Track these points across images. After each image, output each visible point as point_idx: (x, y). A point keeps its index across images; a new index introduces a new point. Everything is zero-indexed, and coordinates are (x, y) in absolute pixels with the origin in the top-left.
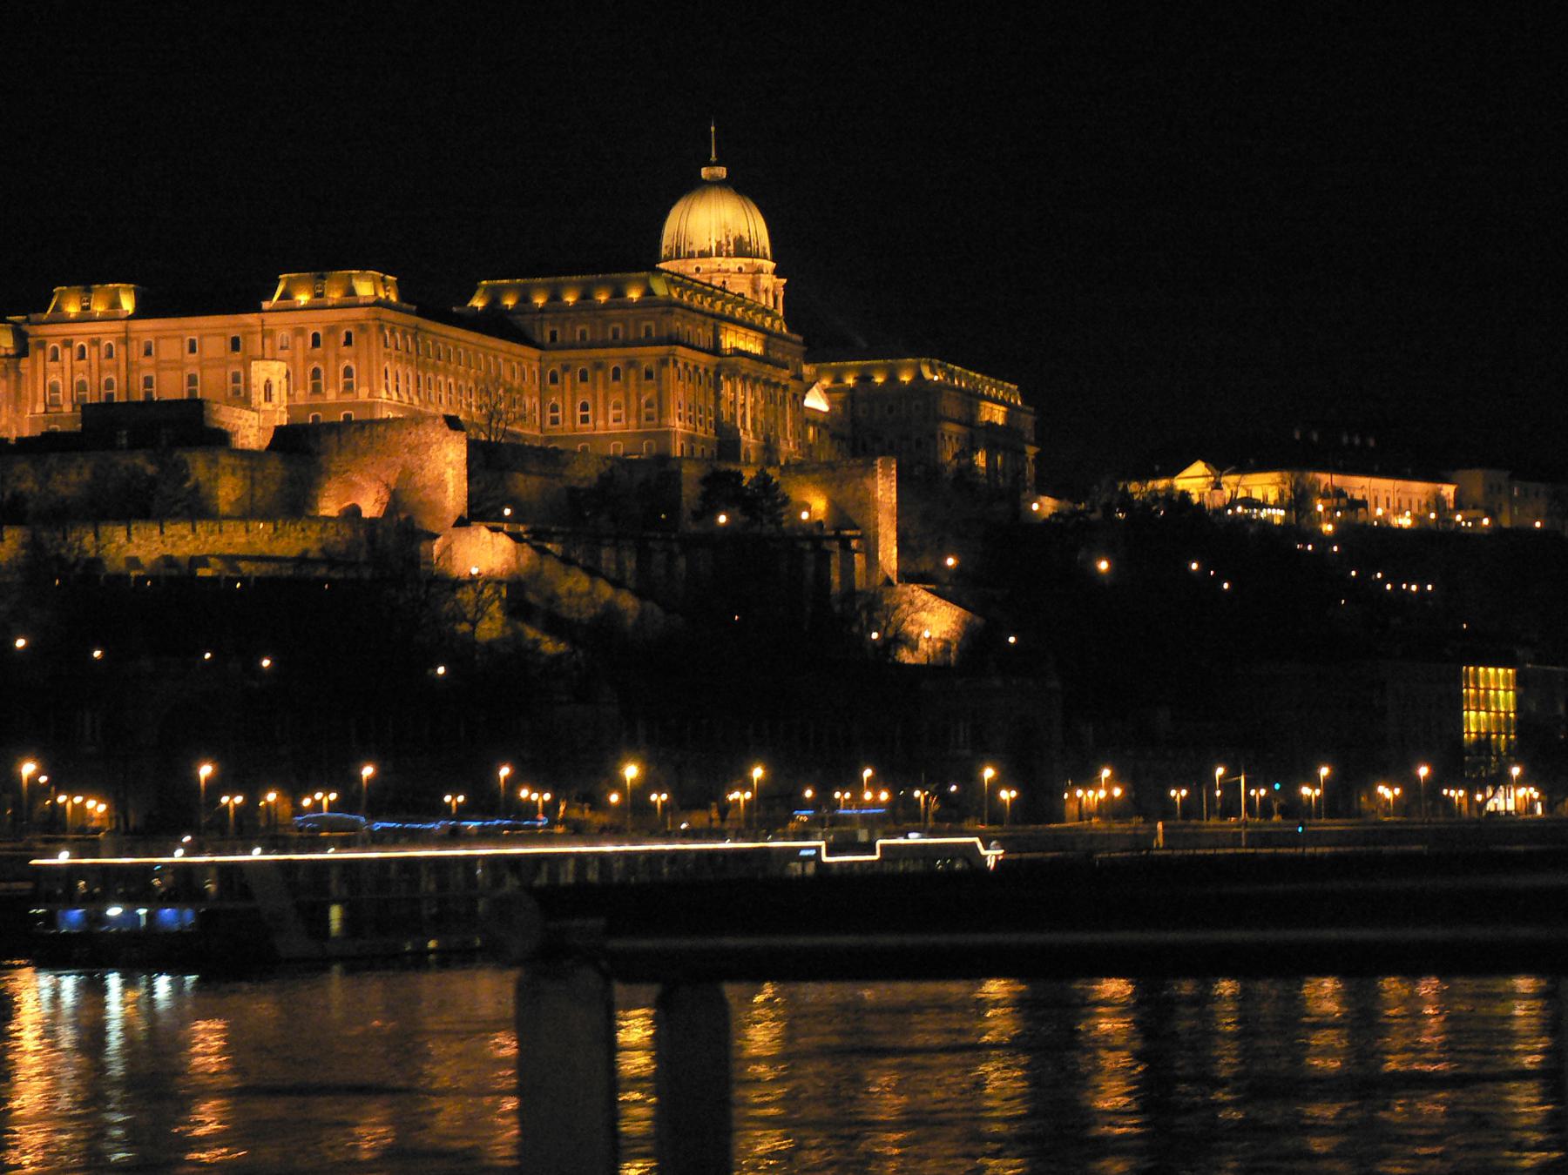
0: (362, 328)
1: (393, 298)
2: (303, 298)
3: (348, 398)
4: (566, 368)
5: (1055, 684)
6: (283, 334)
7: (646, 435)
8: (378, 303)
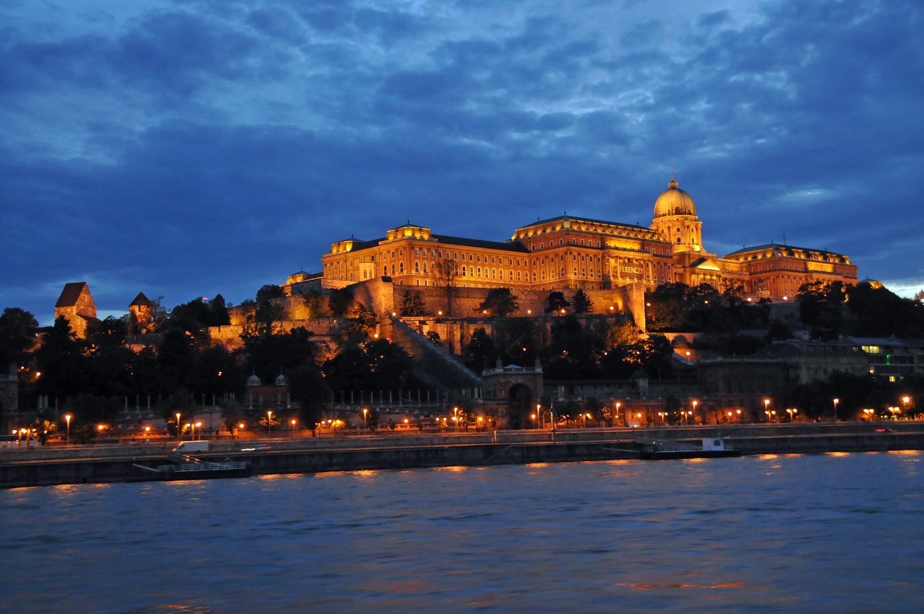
0: (405, 248)
1: (426, 237)
2: (391, 238)
3: (401, 275)
4: (537, 259)
5: (539, 370)
6: (384, 253)
7: (562, 282)
8: (413, 238)
